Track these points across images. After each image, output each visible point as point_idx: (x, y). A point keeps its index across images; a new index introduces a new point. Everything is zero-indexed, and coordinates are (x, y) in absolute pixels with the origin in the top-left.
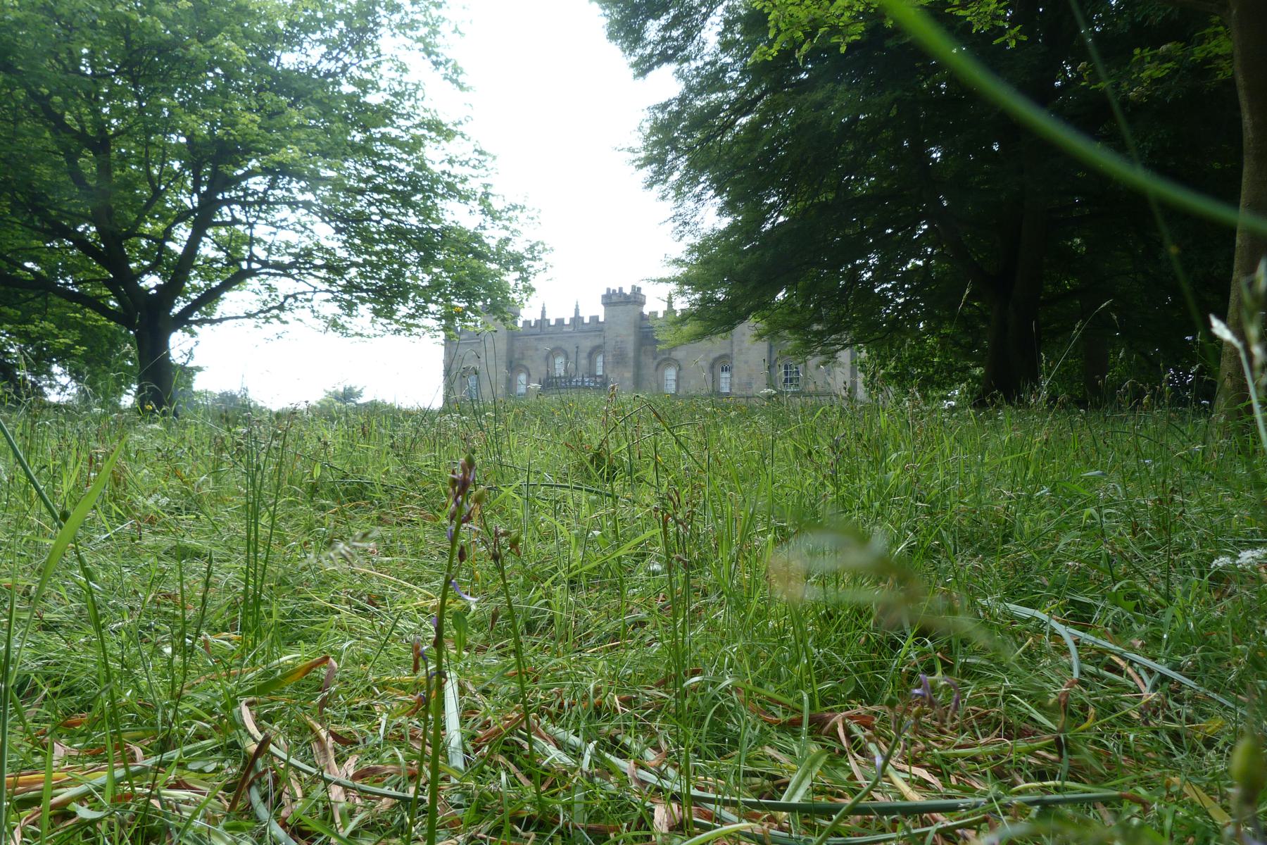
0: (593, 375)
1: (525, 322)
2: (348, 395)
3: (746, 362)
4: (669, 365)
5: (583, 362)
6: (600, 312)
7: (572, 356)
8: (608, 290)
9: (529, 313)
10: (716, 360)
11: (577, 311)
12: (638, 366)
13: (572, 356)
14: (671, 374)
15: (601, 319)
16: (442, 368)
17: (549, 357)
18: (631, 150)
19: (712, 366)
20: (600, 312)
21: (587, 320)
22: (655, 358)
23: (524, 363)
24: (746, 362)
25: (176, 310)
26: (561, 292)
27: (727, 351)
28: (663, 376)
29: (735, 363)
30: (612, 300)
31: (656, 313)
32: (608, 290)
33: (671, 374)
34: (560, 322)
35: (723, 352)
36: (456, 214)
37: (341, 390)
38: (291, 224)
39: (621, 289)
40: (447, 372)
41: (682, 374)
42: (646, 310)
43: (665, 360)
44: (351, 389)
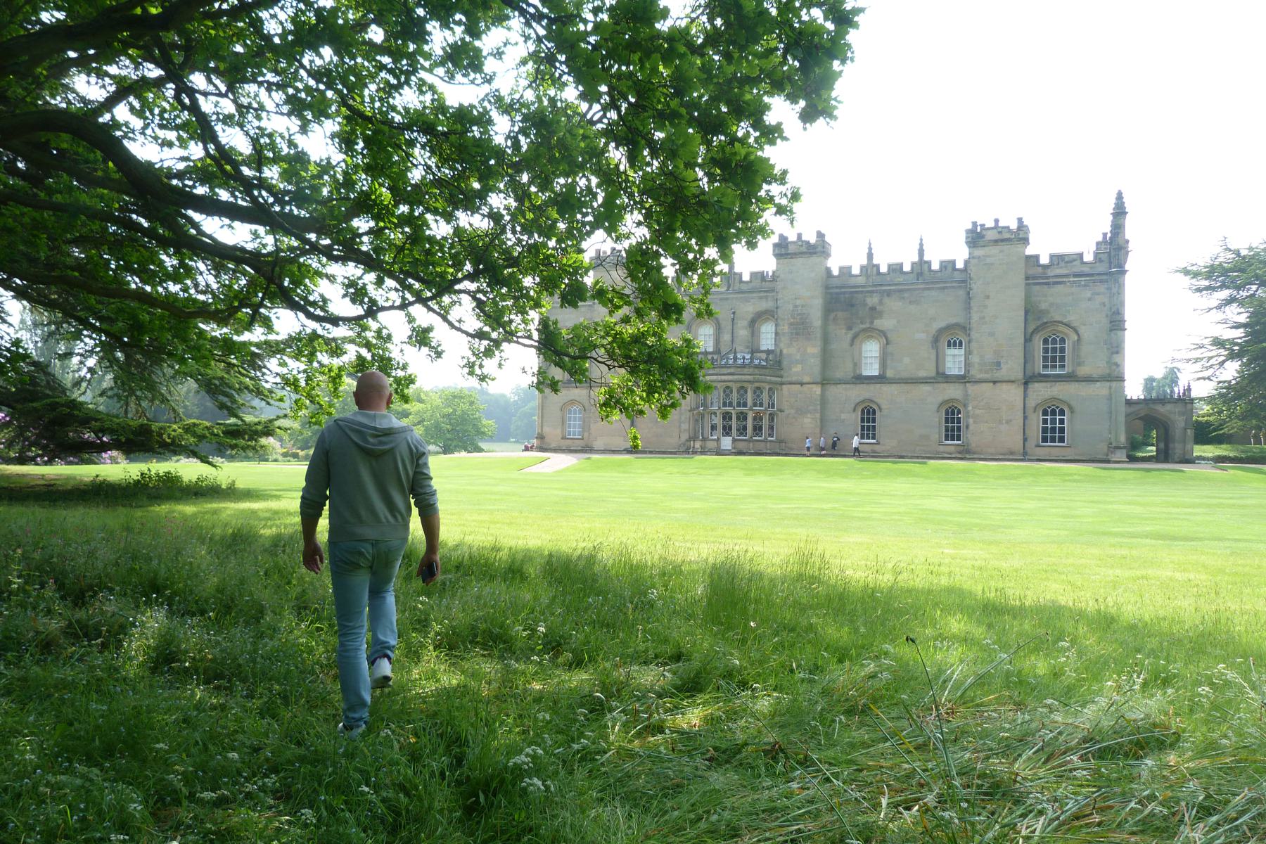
0: (754, 351)
3: (992, 334)
4: (870, 337)
5: (743, 333)
6: (960, 254)
7: (727, 325)
8: (975, 224)
10: (941, 331)
11: (870, 256)
12: (826, 340)
13: (727, 325)
14: (871, 349)
19: (936, 341)
22: (850, 328)
24: (992, 334)
25: (308, 236)
27: (959, 319)
28: (860, 353)
29: (974, 335)
31: (953, 262)
32: (975, 224)
33: (871, 349)
35: (953, 320)
41: (890, 348)
43: (864, 330)
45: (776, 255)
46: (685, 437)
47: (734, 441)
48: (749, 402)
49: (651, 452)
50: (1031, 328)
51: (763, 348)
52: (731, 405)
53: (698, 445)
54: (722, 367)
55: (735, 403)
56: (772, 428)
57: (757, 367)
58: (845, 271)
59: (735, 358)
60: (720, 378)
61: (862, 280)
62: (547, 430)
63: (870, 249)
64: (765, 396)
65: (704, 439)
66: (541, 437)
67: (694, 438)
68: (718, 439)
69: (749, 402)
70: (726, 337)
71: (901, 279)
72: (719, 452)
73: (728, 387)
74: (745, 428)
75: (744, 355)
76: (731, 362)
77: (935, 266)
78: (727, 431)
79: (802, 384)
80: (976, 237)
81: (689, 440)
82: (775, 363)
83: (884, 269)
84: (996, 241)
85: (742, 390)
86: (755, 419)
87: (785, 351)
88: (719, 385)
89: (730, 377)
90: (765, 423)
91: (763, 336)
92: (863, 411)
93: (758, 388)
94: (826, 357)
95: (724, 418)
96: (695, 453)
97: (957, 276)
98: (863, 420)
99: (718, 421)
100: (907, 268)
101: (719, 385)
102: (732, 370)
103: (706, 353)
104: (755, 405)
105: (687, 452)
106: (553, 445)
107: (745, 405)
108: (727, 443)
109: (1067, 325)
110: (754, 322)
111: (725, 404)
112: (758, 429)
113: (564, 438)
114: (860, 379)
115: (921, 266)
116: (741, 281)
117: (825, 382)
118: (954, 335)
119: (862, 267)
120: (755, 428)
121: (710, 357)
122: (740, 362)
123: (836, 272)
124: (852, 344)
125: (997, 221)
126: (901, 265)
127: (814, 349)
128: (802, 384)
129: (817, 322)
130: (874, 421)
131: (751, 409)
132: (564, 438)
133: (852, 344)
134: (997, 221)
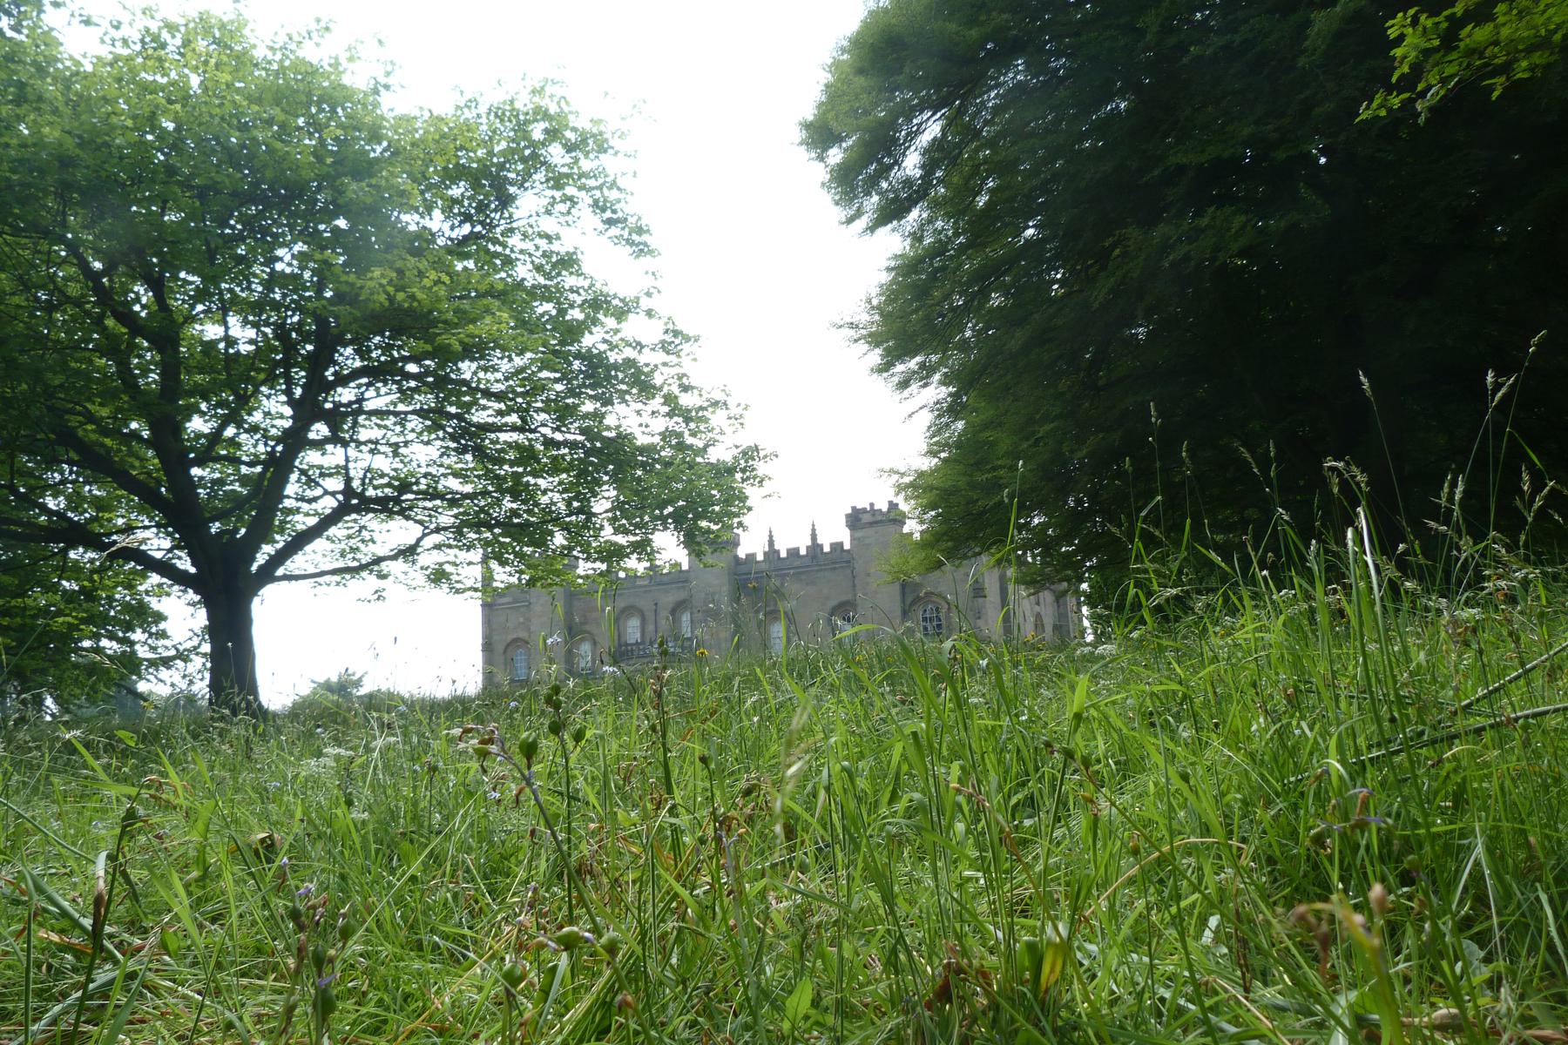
2: (343, 687)
5: (664, 624)
9: (751, 544)
13: (650, 616)
15: (847, 546)
18: (852, 326)
21: (827, 549)
23: (587, 628)
26: (789, 514)
27: (850, 597)
35: (844, 598)
36: (637, 421)
38: (391, 439)
40: (488, 647)
50: (909, 599)
58: (751, 557)
61: (764, 567)
63: (814, 530)
70: (651, 628)
71: (797, 563)
77: (827, 549)
80: (855, 519)
83: (783, 554)
84: (871, 524)
97: (846, 557)
100: (803, 552)
109: (939, 595)
110: (677, 609)
115: (815, 547)
118: (845, 610)
125: (872, 505)
126: (797, 549)
134: (872, 505)
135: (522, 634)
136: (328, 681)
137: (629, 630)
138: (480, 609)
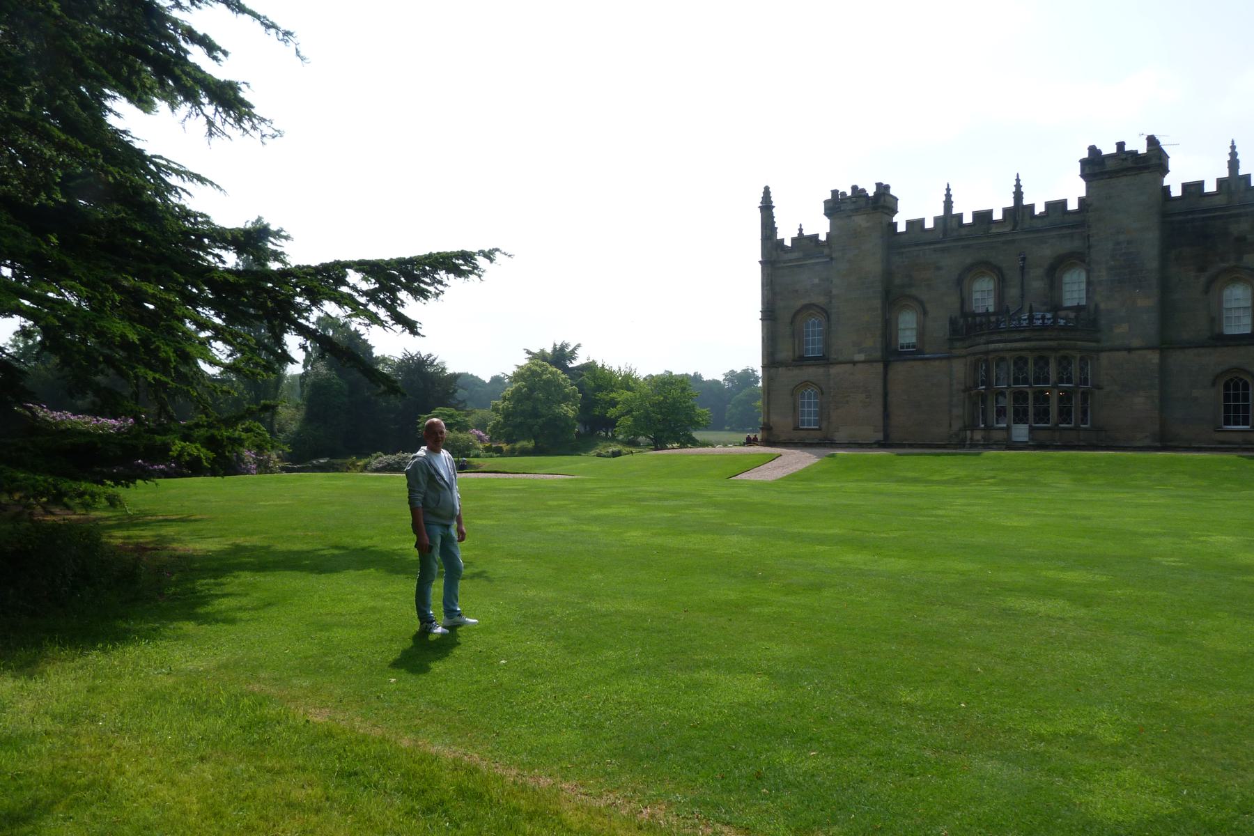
0: (1056, 308)
1: (910, 224)
2: (560, 356)
5: (1037, 284)
12: (1165, 287)
16: (759, 307)
17: (961, 282)
20: (1073, 191)
22: (1202, 269)
28: (1220, 302)
30: (1095, 167)
34: (983, 217)
37: (549, 350)
39: (1121, 145)
40: (770, 314)
42: (1174, 182)
44: (563, 347)
45: (1083, 176)
46: (957, 425)
47: (1032, 430)
48: (1053, 376)
49: (911, 446)
51: (1067, 304)
52: (1026, 381)
53: (978, 436)
54: (1011, 331)
55: (1032, 380)
56: (1085, 413)
57: (1063, 328)
58: (1193, 189)
59: (1031, 318)
60: (1009, 345)
61: (1221, 201)
62: (774, 419)
64: (1075, 370)
65: (988, 428)
66: (767, 428)
67: (973, 427)
68: (1008, 429)
69: (1053, 376)
70: (1013, 292)
72: (1011, 445)
73: (1020, 358)
74: (1069, 413)
75: (1043, 316)
76: (1025, 324)
78: (1020, 417)
79: (1129, 350)
81: (965, 428)
82: (1087, 321)
85: (1042, 361)
86: (1061, 399)
87: (1102, 306)
88: (1007, 355)
89: (1024, 344)
90: (1076, 402)
91: (1066, 288)
92: (1227, 387)
93: (1065, 358)
94: (1166, 310)
95: (1016, 400)
96: (974, 445)
98: (1227, 397)
99: (1007, 402)
101: (1007, 355)
102: (1026, 335)
103: (987, 314)
104: (1061, 381)
105: (961, 444)
106: (783, 438)
107: (1046, 380)
108: (1021, 432)
111: (1016, 381)
112: (1065, 414)
113: (796, 429)
114: (1222, 340)
116: (1033, 216)
117: (1165, 345)
119: (1220, 182)
120: (1061, 412)
121: (993, 319)
122: (1039, 322)
123: (1176, 192)
124: (1207, 289)
127: (1146, 301)
128: (1129, 350)
129: (1153, 264)
130: (1246, 398)
131: (1055, 386)
132: (796, 429)
133: (1207, 289)
135: (820, 300)
136: (543, 351)
137: (977, 296)
138: (759, 267)
